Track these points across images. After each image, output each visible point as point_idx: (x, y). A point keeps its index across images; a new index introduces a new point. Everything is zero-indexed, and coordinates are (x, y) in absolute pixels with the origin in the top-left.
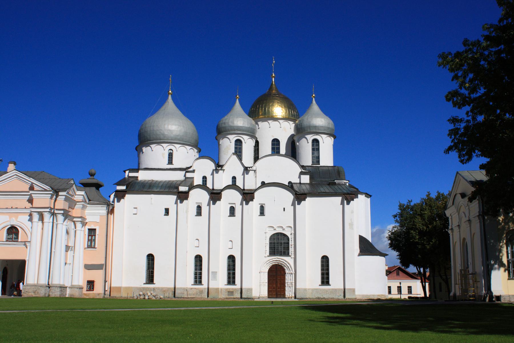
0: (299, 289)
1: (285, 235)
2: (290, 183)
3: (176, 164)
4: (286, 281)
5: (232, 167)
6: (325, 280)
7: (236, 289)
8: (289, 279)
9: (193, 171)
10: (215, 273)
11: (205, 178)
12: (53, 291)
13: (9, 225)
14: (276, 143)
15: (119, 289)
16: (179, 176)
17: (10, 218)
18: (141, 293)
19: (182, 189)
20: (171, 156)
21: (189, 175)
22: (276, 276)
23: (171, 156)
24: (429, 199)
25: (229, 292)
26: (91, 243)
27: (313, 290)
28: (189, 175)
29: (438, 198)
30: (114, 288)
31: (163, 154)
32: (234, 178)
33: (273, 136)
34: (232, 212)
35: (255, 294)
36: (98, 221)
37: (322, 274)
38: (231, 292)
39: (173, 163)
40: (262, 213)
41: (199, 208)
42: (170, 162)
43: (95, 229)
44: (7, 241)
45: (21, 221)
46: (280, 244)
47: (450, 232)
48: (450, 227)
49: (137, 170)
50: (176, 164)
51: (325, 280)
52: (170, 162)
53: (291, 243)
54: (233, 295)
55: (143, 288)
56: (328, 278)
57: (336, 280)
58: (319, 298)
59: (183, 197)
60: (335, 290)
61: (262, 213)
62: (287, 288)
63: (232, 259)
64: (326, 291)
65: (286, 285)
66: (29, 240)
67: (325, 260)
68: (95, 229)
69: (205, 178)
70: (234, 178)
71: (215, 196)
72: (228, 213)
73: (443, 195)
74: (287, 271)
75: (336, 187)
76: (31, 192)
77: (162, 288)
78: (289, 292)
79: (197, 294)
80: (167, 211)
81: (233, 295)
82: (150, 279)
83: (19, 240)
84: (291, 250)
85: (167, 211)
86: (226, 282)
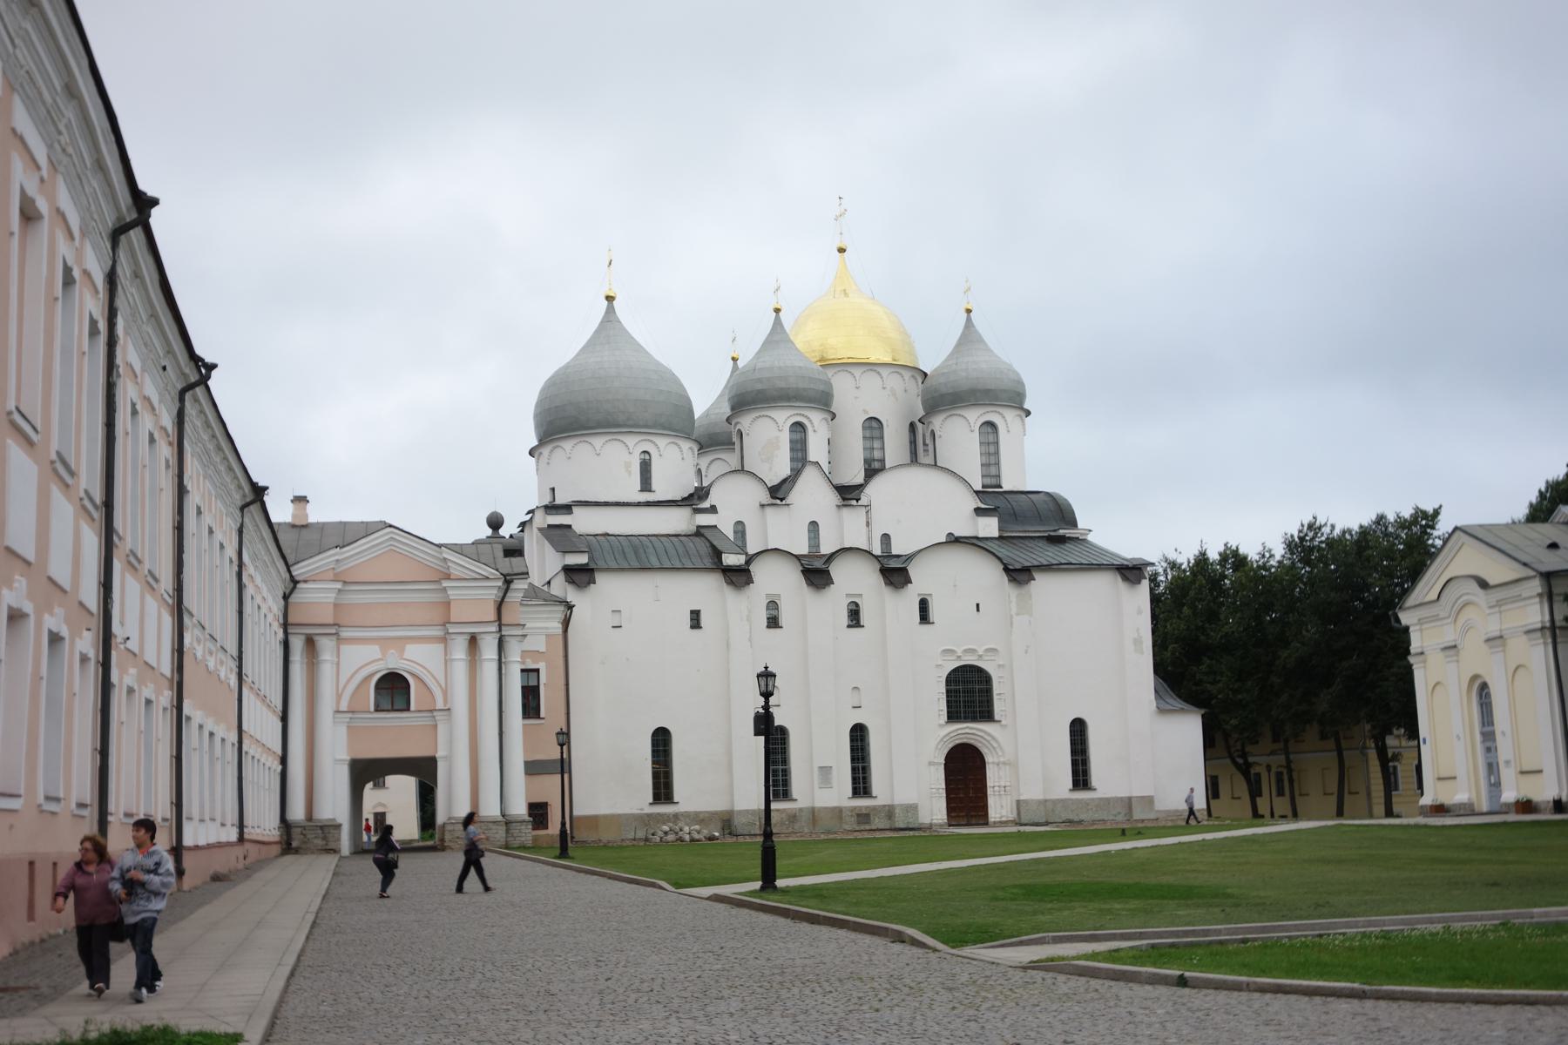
0: (1026, 801)
1: (980, 670)
2: (950, 534)
3: (661, 491)
4: (989, 783)
5: (813, 496)
6: (1081, 779)
7: (874, 808)
8: (994, 777)
9: (713, 510)
10: (825, 771)
11: (740, 528)
12: (516, 832)
13: (382, 668)
14: (873, 426)
15: (593, 821)
16: (676, 521)
17: (384, 652)
18: (666, 828)
19: (731, 560)
20: (646, 468)
21: (704, 520)
22: (965, 773)
23: (646, 468)
24: (1202, 560)
25: (858, 815)
26: (531, 705)
27: (1055, 802)
28: (704, 520)
29: (1224, 557)
30: (581, 818)
31: (628, 465)
32: (814, 525)
33: (865, 412)
34: (854, 616)
35: (925, 818)
36: (543, 649)
37: (1074, 763)
38: (863, 817)
39: (654, 487)
40: (924, 616)
41: (773, 605)
42: (646, 485)
43: (537, 671)
44: (377, 710)
45: (419, 660)
46: (969, 693)
47: (1411, 659)
48: (1414, 647)
49: (567, 508)
50: (664, 487)
51: (1081, 779)
52: (646, 485)
53: (997, 688)
54: (868, 822)
55: (649, 815)
56: (1086, 773)
57: (1108, 780)
58: (1070, 822)
59: (739, 577)
60: (1108, 800)
61: (924, 616)
62: (991, 801)
63: (859, 735)
64: (1086, 803)
65: (989, 791)
66: (440, 705)
67: (1078, 729)
68: (537, 671)
69: (740, 528)
70: (814, 525)
71: (816, 574)
72: (844, 618)
73: (1235, 553)
74: (989, 759)
75: (1068, 546)
76: (445, 584)
77: (697, 814)
78: (999, 808)
79: (782, 824)
80: (695, 619)
81: (868, 822)
82: (663, 789)
83: (413, 707)
84: (998, 707)
85: (695, 619)
86: (850, 793)
